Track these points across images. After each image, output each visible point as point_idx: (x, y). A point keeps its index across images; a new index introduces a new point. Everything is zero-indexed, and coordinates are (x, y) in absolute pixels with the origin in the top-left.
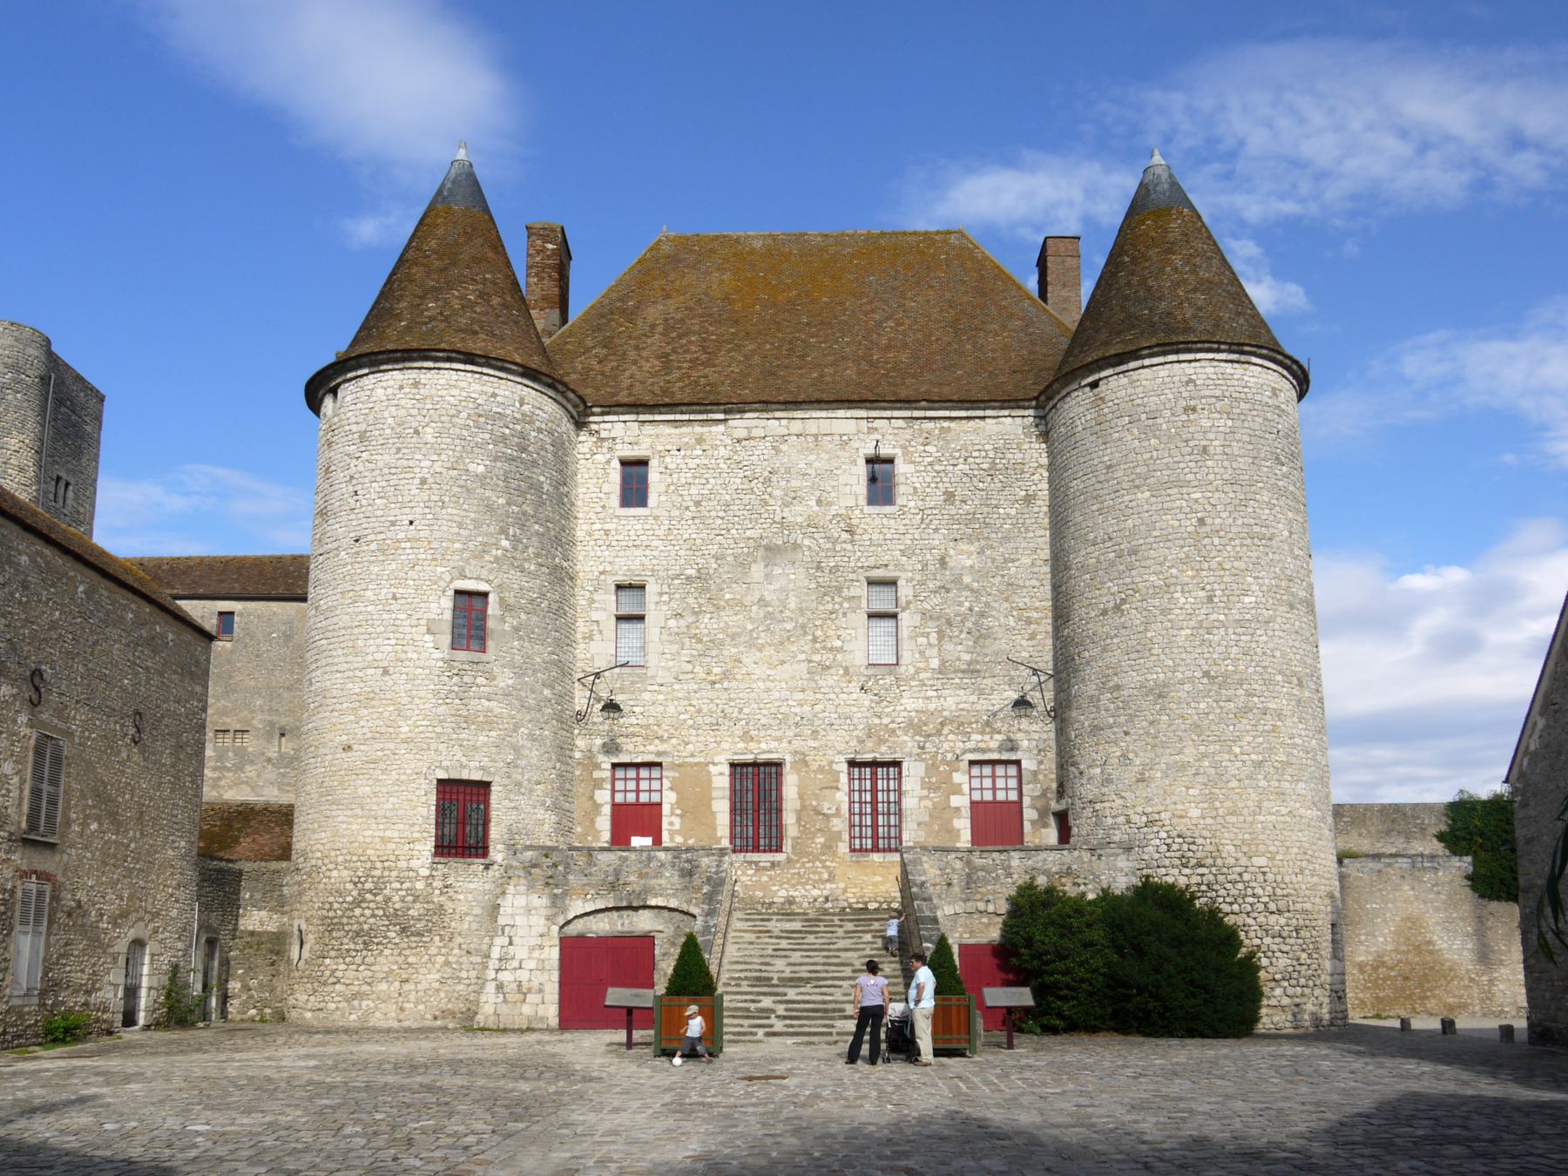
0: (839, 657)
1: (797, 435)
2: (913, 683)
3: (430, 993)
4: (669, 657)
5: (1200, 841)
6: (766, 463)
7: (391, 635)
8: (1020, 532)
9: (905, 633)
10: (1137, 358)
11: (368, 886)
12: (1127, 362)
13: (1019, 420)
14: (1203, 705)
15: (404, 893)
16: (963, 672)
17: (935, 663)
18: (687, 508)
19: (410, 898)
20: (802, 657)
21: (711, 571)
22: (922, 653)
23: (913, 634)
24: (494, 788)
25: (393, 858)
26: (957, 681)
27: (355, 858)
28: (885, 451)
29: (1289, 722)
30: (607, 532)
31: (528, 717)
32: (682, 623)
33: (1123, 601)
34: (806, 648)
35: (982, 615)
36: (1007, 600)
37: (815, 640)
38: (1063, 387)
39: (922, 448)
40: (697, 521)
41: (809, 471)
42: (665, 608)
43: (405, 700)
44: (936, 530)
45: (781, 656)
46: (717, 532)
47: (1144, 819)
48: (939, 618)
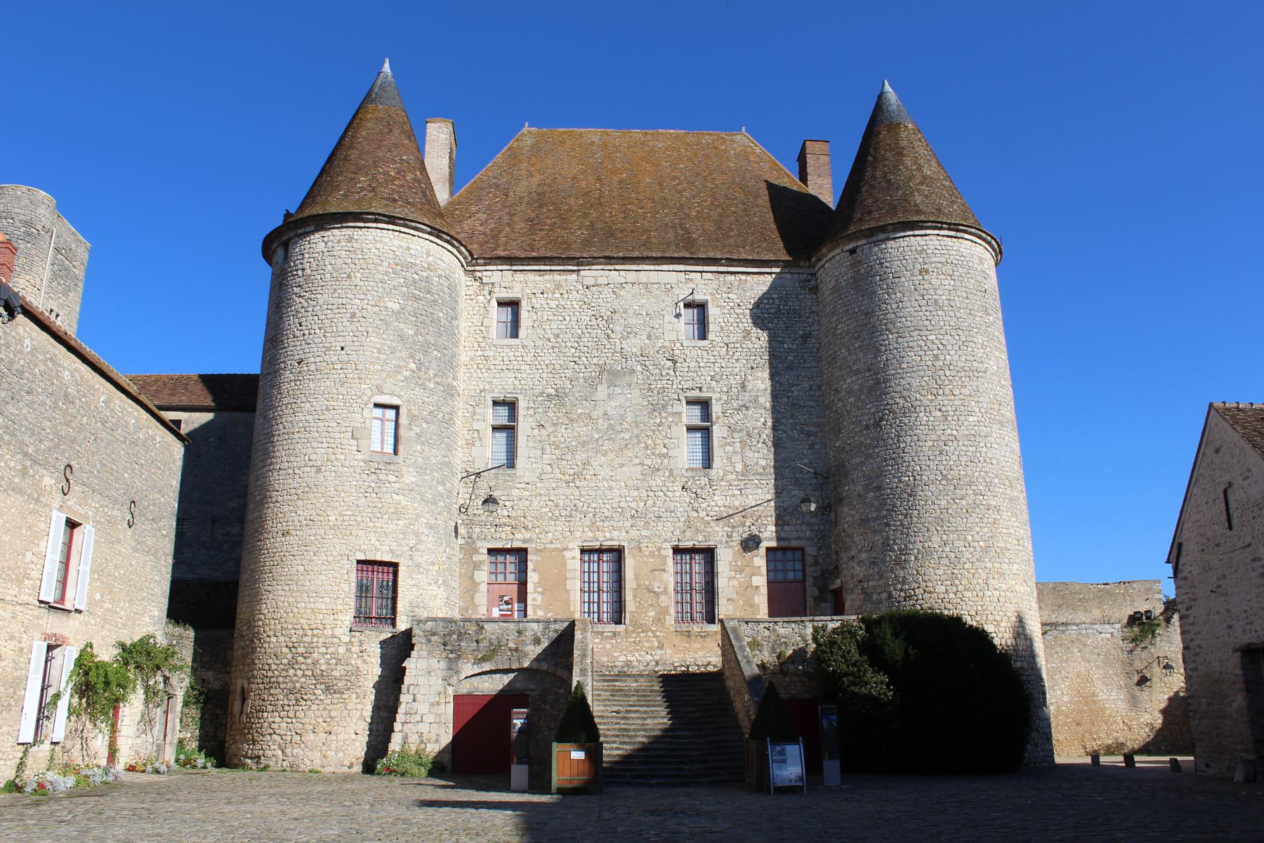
0: (666, 461)
1: (633, 284)
2: (722, 484)
3: (348, 742)
4: (533, 460)
6: (609, 305)
7: (324, 440)
8: (800, 363)
10: (884, 232)
11: (301, 650)
12: (877, 236)
13: (796, 276)
14: (943, 503)
15: (329, 656)
16: (760, 474)
17: (739, 467)
18: (549, 340)
19: (334, 661)
20: (637, 461)
21: (567, 390)
22: (729, 459)
23: (721, 443)
24: (401, 569)
25: (321, 627)
26: (757, 482)
27: (290, 627)
28: (699, 297)
30: (486, 358)
31: (427, 509)
32: (544, 432)
33: (881, 419)
34: (639, 454)
36: (792, 416)
37: (647, 447)
38: (830, 251)
39: (726, 295)
40: (556, 350)
41: (641, 312)
42: (530, 420)
43: (333, 493)
44: (737, 360)
45: (619, 460)
46: (572, 359)
47: (903, 594)
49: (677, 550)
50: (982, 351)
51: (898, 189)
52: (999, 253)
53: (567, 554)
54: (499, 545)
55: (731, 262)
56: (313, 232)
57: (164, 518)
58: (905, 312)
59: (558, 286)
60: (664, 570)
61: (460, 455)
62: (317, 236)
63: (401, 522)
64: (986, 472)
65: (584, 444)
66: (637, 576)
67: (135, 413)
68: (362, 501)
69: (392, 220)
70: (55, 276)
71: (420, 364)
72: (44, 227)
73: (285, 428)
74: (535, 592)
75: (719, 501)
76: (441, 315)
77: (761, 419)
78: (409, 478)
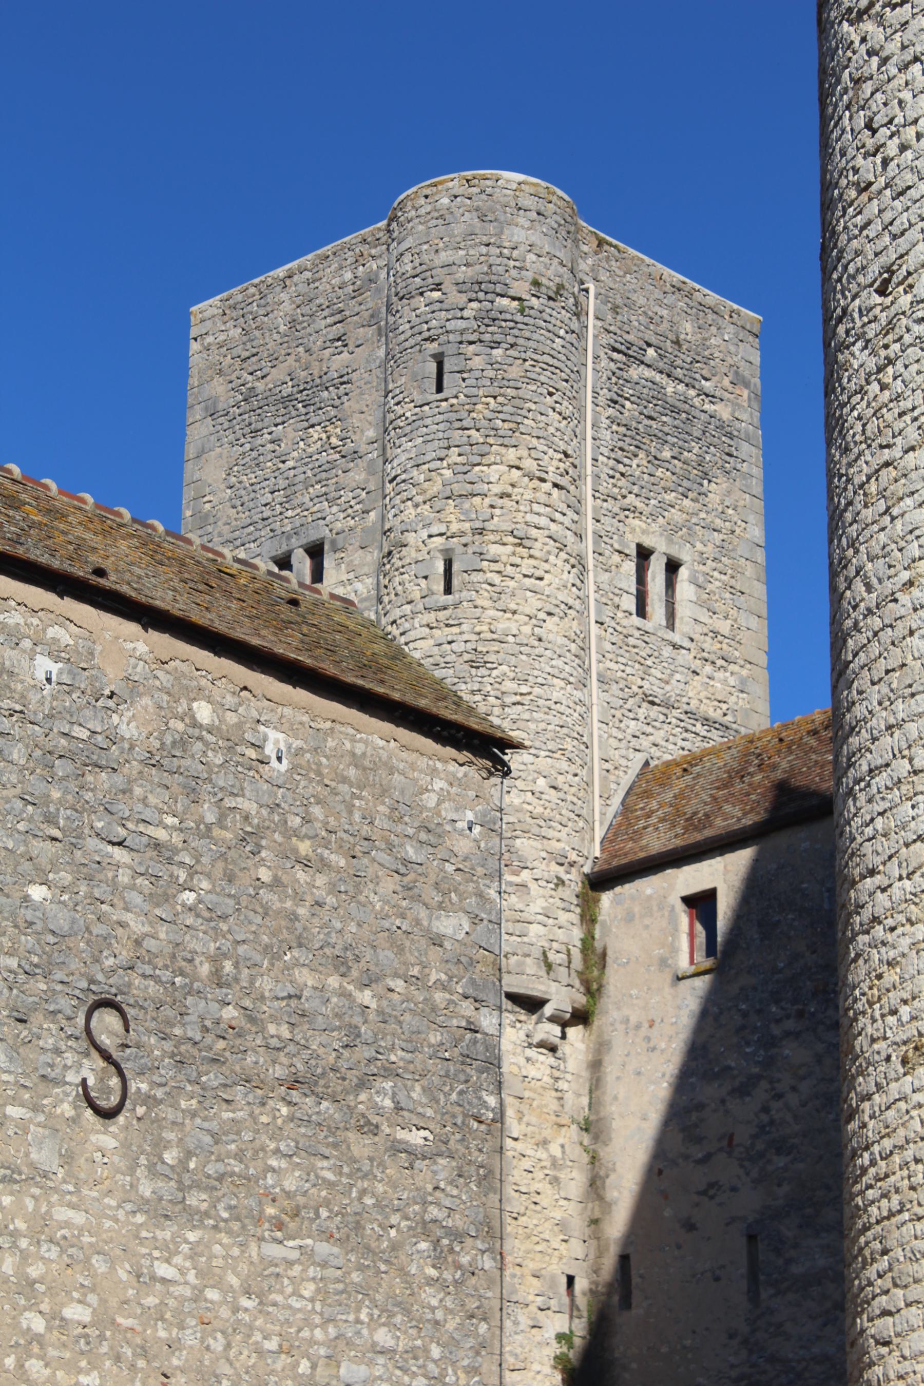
57: (390, 1072)
67: (52, 632)
72: (536, 283)
73: (869, 588)
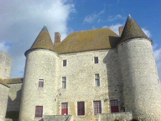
5: (142, 111)
9: (100, 81)
17: (105, 85)
20: (86, 86)
29: (154, 91)
35: (111, 78)
36: (114, 75)
38: (119, 45)
47: (134, 108)
48: (105, 79)
49: (94, 101)
50: (147, 60)
51: (130, 32)
52: (151, 41)
53: (75, 103)
54: (63, 102)
55: (102, 49)
56: (30, 52)
58: (131, 54)
59: (73, 57)
60: (92, 105)
61: (57, 87)
62: (31, 53)
63: (43, 99)
64: (149, 83)
65: (77, 83)
66: (87, 106)
68: (37, 96)
69: (42, 49)
70: (6, 64)
71: (47, 72)
74: (69, 110)
75: (101, 92)
76: (52, 63)
77: (106, 77)
78: (45, 91)
